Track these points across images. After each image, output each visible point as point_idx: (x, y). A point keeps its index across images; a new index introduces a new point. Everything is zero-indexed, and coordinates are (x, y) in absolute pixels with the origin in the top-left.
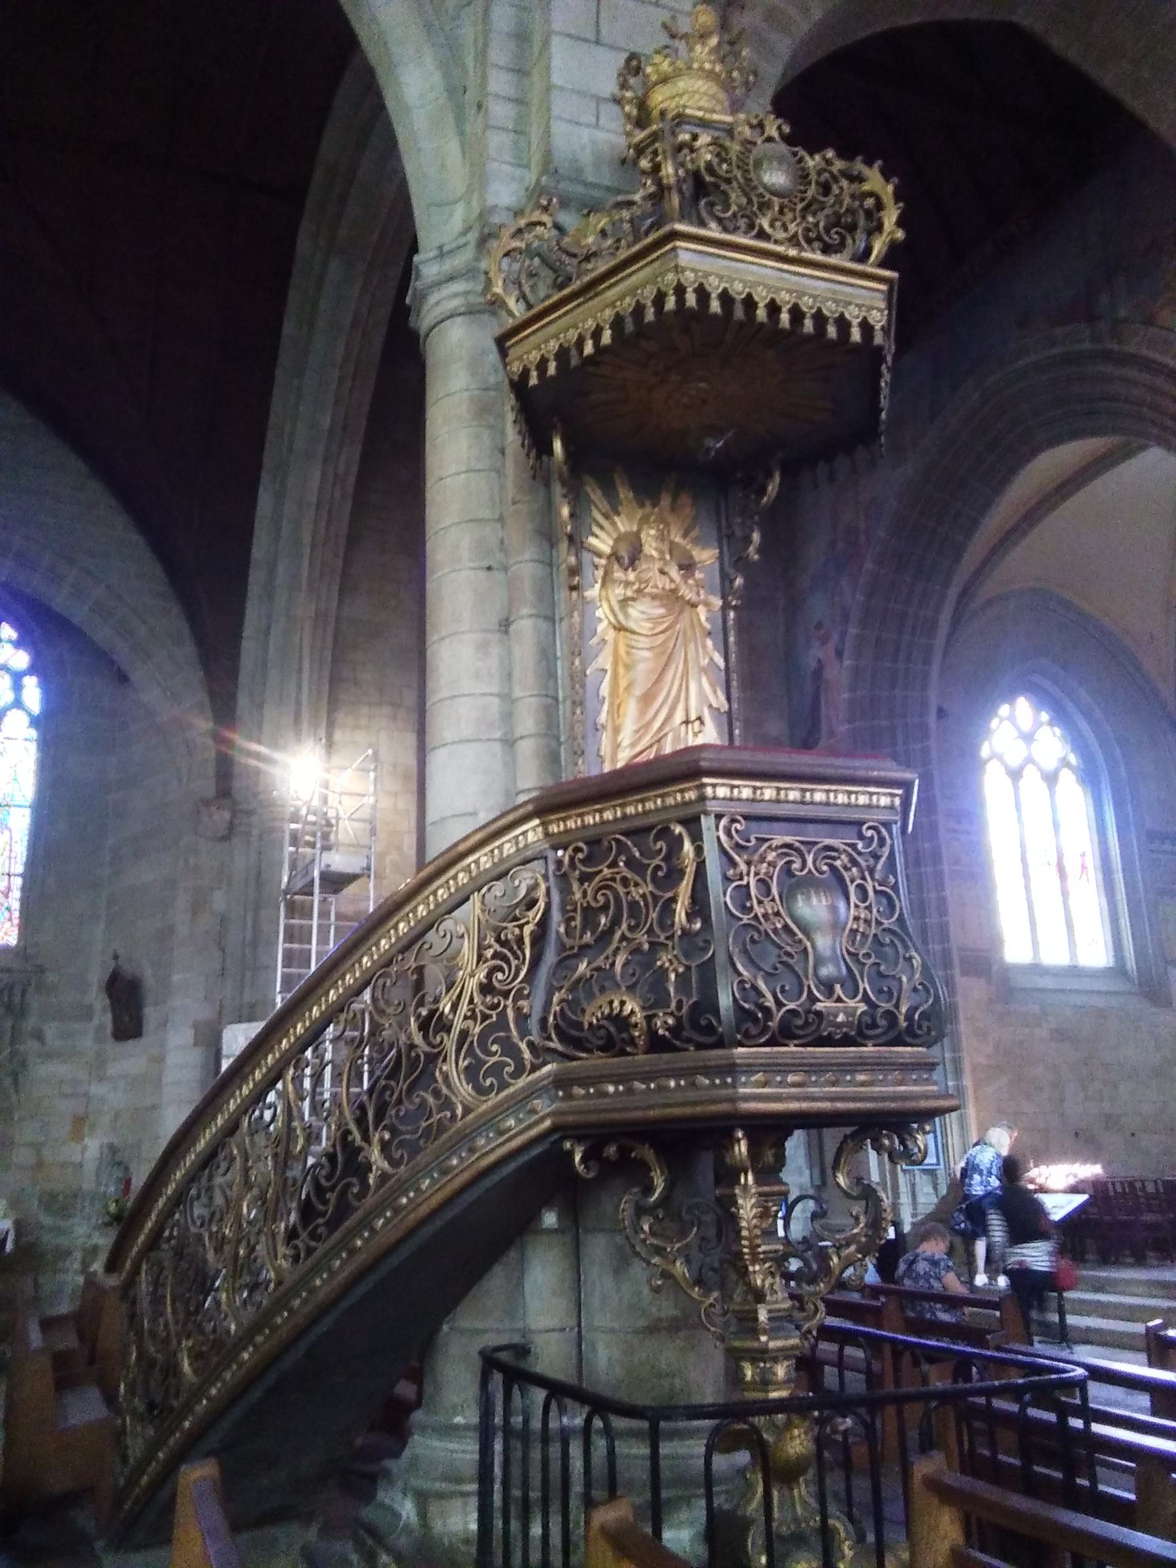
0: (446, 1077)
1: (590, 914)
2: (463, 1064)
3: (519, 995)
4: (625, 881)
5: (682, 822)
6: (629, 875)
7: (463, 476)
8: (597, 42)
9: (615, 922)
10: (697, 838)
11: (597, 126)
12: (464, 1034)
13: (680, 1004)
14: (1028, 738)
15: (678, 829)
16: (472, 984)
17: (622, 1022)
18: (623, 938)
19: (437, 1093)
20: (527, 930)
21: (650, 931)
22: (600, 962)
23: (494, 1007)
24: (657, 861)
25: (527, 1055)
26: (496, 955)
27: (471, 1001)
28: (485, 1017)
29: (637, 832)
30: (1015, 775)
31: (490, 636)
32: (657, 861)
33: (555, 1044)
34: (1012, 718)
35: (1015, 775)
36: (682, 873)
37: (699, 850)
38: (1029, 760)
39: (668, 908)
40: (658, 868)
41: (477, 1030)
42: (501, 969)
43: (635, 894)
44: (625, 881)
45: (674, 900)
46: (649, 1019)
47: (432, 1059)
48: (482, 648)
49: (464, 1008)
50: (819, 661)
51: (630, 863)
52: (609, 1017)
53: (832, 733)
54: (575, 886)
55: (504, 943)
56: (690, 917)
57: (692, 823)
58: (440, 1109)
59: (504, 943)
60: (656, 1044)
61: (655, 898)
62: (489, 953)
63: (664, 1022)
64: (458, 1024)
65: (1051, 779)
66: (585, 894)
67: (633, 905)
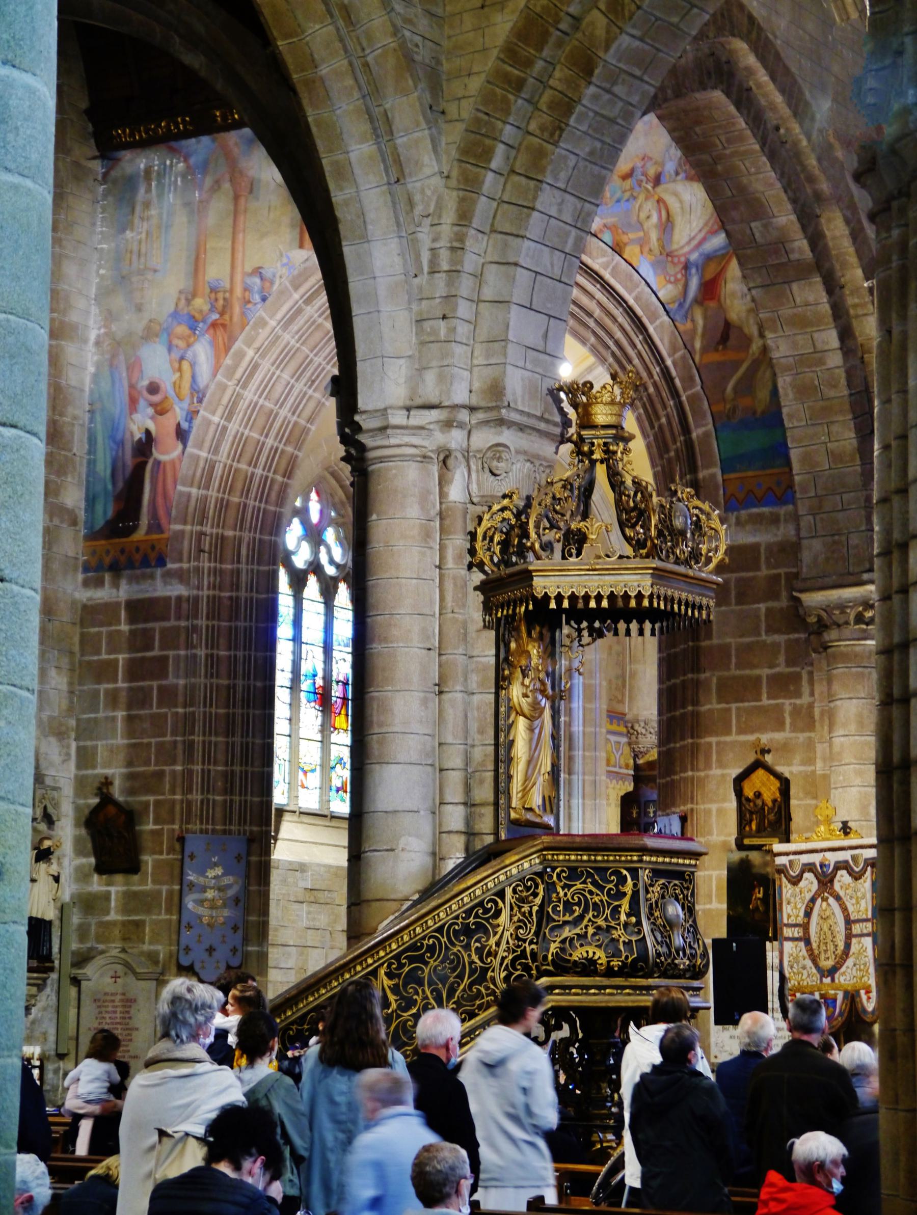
0: (493, 980)
1: (568, 906)
2: (503, 975)
3: (531, 943)
4: (591, 893)
5: (627, 869)
6: (594, 890)
7: (414, 581)
8: (530, 309)
9: (586, 910)
10: (635, 877)
11: (524, 369)
12: (503, 959)
13: (627, 957)
14: (314, 536)
15: (625, 872)
16: (507, 934)
17: (592, 962)
18: (590, 920)
19: (487, 988)
20: (535, 909)
21: (606, 920)
22: (578, 931)
23: (519, 946)
24: (611, 886)
25: (534, 972)
26: (519, 921)
27: (508, 943)
28: (514, 951)
29: (602, 871)
30: (298, 581)
31: (428, 695)
32: (611, 886)
33: (551, 968)
34: (303, 513)
35: (298, 581)
36: (625, 894)
37: (635, 885)
38: (316, 568)
39: (616, 911)
40: (611, 889)
41: (511, 957)
42: (520, 927)
43: (597, 899)
44: (591, 893)
45: (620, 906)
46: (609, 962)
47: (485, 971)
48: (425, 702)
49: (503, 946)
50: (148, 432)
51: (595, 883)
52: (586, 959)
53: (156, 526)
54: (559, 889)
55: (524, 914)
56: (628, 915)
57: (634, 872)
58: (488, 995)
59: (524, 914)
60: (609, 972)
61: (609, 904)
62: (515, 919)
63: (615, 963)
64: (501, 954)
65: (328, 592)
66: (566, 895)
67: (595, 904)
